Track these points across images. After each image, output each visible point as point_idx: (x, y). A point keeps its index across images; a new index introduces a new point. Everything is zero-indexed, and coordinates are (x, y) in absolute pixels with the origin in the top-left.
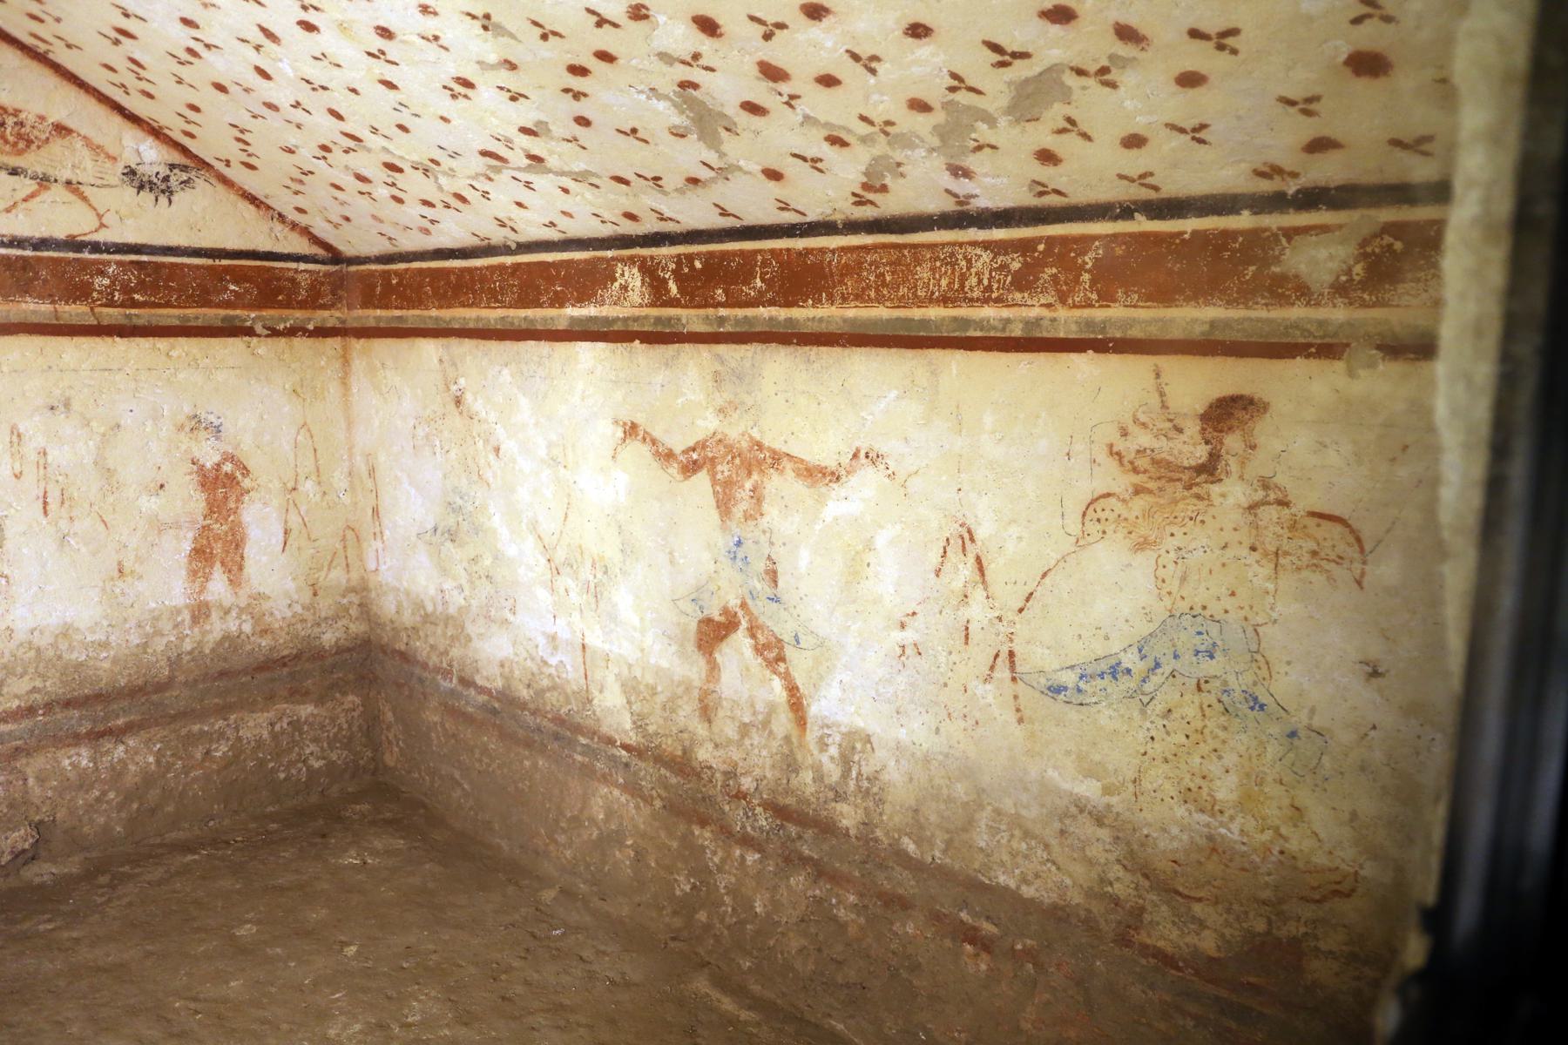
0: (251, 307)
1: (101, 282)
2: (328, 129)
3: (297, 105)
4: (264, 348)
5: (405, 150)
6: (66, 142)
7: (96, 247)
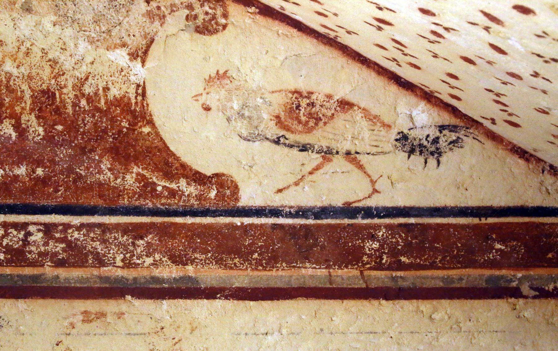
0: (517, 266)
1: (372, 246)
4: (531, 310)
6: (348, 116)
7: (368, 212)
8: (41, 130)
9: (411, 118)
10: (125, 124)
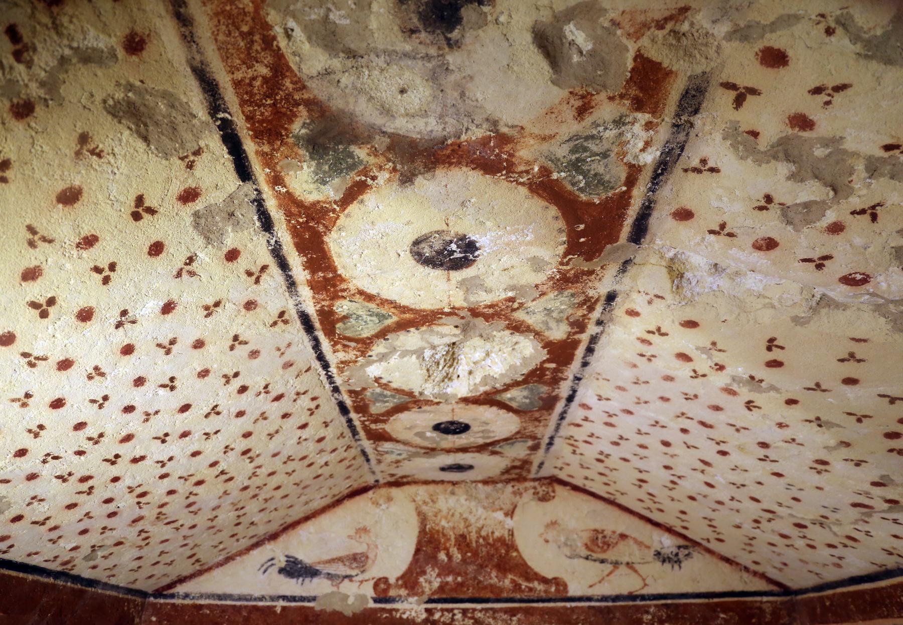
2: (754, 510)
3: (732, 499)
5: (804, 513)
7: (643, 598)
8: (459, 556)
9: (661, 542)
10: (503, 551)
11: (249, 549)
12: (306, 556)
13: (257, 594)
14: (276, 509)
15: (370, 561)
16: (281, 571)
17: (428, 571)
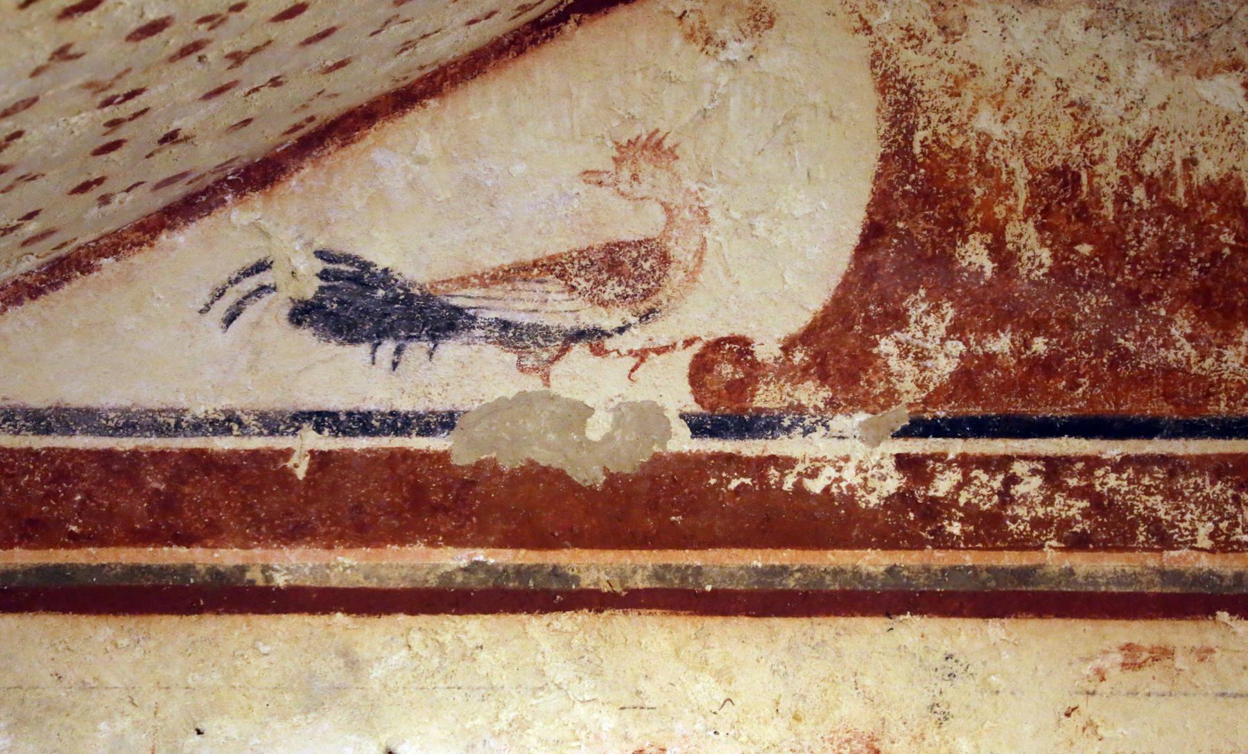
8: (1045, 255)
11: (151, 228)
12: (408, 252)
13: (201, 408)
14: (275, 82)
15: (676, 275)
16: (301, 314)
17: (913, 314)
